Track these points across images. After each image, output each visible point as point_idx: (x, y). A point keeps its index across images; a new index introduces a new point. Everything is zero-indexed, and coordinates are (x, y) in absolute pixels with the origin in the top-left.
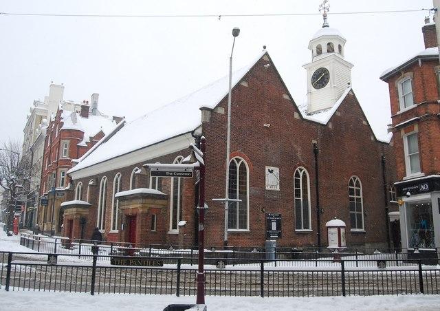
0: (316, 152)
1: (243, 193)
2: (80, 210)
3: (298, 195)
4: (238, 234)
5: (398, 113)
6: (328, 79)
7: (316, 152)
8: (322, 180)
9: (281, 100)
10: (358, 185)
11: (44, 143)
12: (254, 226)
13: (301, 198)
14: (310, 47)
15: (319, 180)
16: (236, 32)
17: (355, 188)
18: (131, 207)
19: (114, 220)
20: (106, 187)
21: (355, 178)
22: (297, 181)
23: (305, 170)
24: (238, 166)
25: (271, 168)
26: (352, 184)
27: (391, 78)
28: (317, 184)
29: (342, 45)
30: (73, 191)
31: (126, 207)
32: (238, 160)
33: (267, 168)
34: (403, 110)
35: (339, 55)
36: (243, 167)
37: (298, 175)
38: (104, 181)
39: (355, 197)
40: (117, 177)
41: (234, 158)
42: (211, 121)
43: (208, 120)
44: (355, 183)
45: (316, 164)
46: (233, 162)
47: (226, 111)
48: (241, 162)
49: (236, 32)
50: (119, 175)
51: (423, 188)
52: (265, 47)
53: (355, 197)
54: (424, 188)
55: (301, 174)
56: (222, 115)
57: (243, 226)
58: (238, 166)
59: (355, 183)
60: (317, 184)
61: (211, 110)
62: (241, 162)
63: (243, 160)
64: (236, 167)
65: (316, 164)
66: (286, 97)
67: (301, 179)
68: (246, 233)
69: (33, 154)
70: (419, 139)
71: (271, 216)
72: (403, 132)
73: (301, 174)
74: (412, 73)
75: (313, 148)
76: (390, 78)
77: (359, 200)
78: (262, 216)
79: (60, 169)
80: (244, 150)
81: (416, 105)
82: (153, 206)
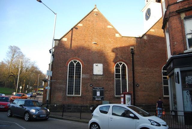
0: (133, 53)
4: (74, 97)
7: (133, 53)
8: (138, 68)
13: (121, 79)
15: (135, 68)
24: (75, 65)
25: (98, 64)
28: (133, 70)
32: (75, 62)
33: (95, 65)
36: (78, 65)
41: (72, 61)
43: (57, 45)
51: (172, 65)
57: (77, 92)
58: (75, 65)
60: (133, 70)
61: (59, 40)
63: (78, 61)
64: (74, 65)
66: (109, 27)
68: (79, 97)
71: (97, 89)
75: (130, 51)
78: (90, 88)
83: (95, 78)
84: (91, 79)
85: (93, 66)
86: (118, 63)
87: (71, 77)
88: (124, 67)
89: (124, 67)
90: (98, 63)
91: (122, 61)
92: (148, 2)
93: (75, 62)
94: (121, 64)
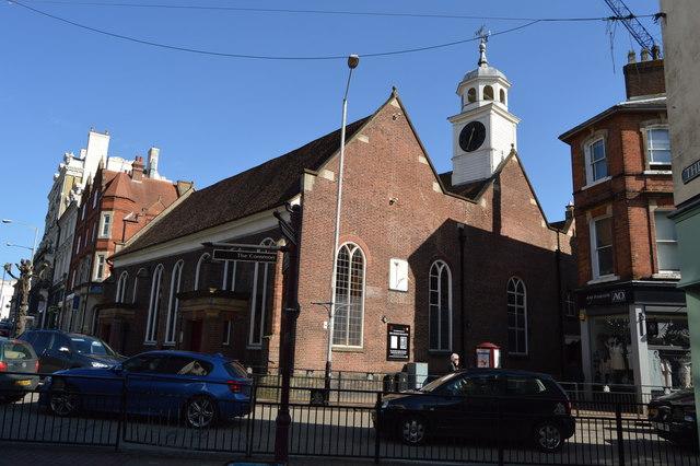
1: (357, 294)
2: (122, 311)
3: (435, 301)
4: (347, 352)
5: (583, 189)
6: (484, 137)
9: (415, 164)
10: (520, 289)
11: (76, 215)
12: (371, 342)
13: (439, 305)
14: (459, 92)
16: (353, 63)
17: (516, 293)
18: (195, 308)
19: (171, 327)
20: (162, 279)
21: (516, 280)
22: (434, 281)
23: (445, 264)
24: (351, 255)
25: (399, 261)
26: (512, 288)
27: (573, 138)
28: (462, 285)
29: (505, 90)
30: (115, 285)
31: (189, 309)
33: (393, 261)
34: (591, 183)
35: (500, 105)
36: (358, 258)
37: (435, 272)
38: (158, 272)
39: (516, 306)
40: (178, 268)
42: (314, 189)
44: (516, 287)
45: (462, 257)
46: (344, 248)
47: (337, 176)
48: (355, 249)
49: (353, 63)
50: (180, 264)
52: (394, 89)
53: (516, 306)
54: (618, 297)
55: (440, 271)
56: (330, 182)
57: (355, 340)
58: (351, 255)
59: (516, 287)
60: (462, 285)
62: (355, 249)
64: (347, 257)
65: (462, 257)
67: (439, 277)
69: (59, 231)
70: (614, 225)
72: (589, 214)
73: (440, 271)
74: (606, 131)
76: (573, 138)
77: (521, 310)
79: (97, 253)
80: (360, 234)
81: (609, 178)
82: (228, 308)
83: (392, 298)
84: (384, 300)
85: (389, 265)
86: (435, 262)
87: (341, 292)
88: (444, 273)
89: (444, 273)
90: (401, 258)
91: (446, 261)
92: (474, 105)
93: (351, 247)
94: (440, 264)
